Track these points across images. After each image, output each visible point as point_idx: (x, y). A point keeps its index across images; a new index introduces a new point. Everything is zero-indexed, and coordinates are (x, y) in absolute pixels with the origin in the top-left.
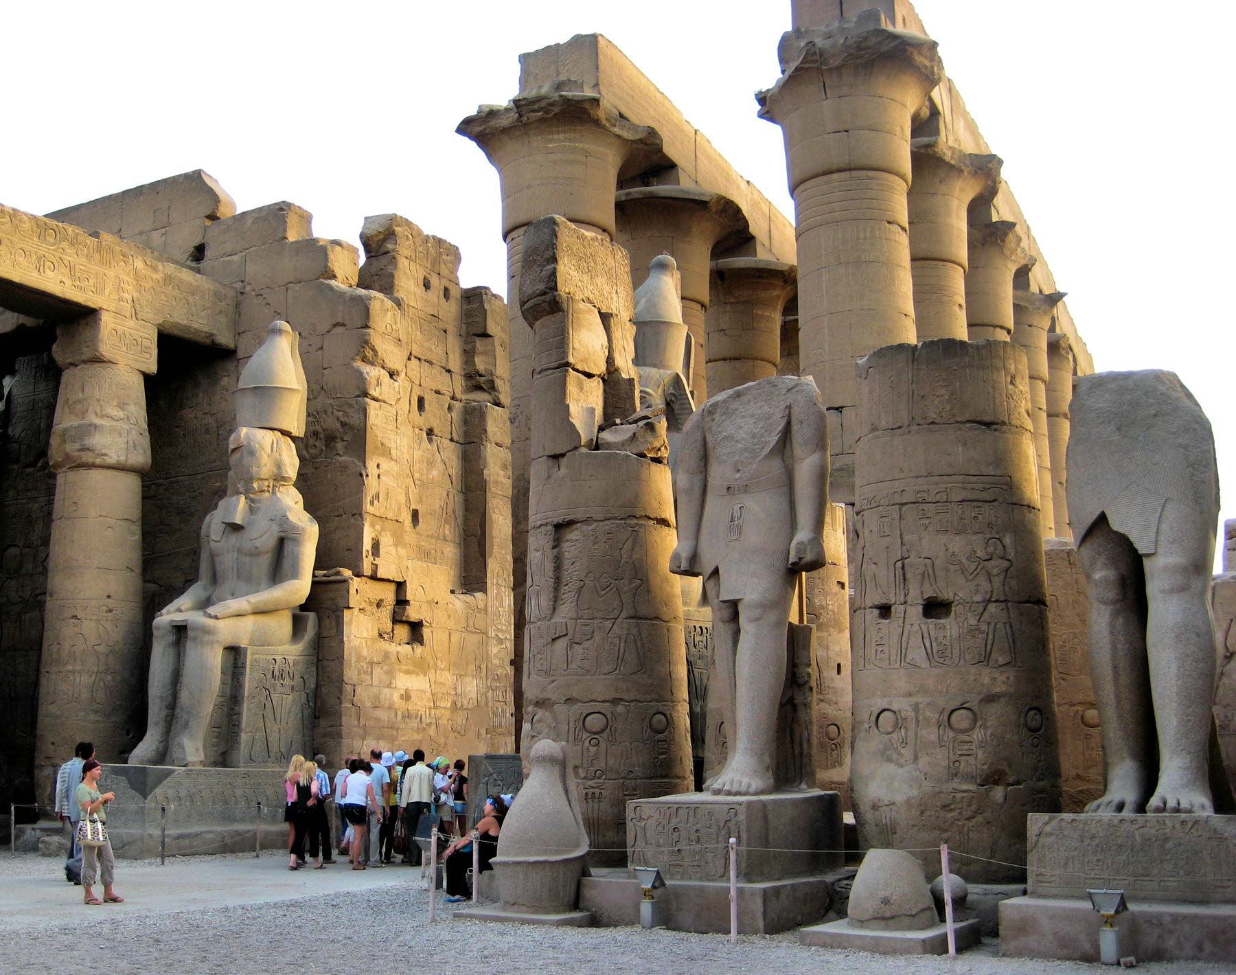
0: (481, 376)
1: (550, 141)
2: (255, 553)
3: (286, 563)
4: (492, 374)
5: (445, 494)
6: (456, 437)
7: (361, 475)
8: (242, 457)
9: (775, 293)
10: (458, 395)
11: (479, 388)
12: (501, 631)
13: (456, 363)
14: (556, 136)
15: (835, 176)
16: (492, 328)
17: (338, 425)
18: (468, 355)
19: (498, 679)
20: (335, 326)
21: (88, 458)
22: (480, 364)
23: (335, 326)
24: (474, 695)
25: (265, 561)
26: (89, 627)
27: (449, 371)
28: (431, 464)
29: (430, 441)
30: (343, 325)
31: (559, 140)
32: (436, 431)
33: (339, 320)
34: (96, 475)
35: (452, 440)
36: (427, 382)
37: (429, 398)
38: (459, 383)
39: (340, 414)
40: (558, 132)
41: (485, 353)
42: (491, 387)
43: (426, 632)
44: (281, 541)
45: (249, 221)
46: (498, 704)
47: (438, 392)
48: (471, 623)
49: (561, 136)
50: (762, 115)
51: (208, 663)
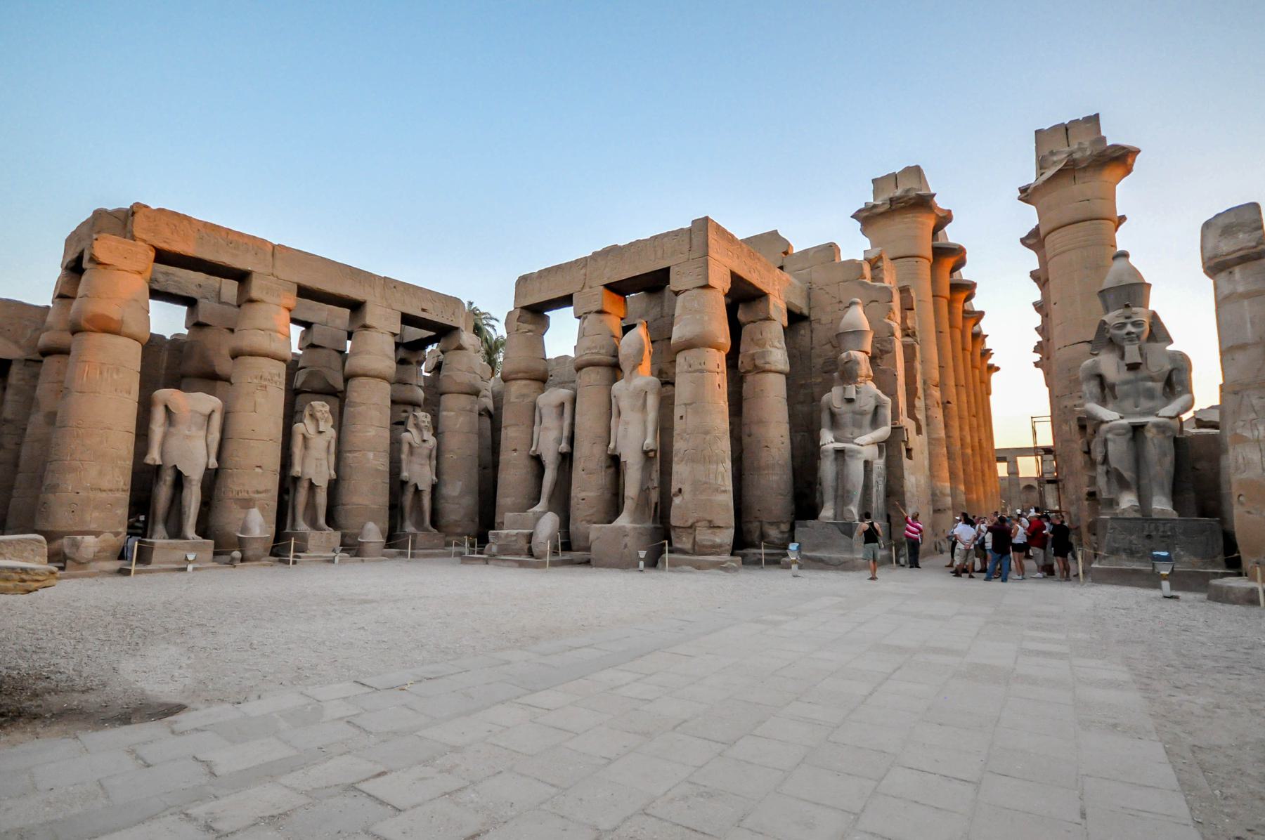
2: (863, 413)
3: (880, 418)
11: (908, 335)
21: (767, 367)
22: (909, 323)
25: (869, 417)
26: (774, 451)
34: (771, 377)
42: (914, 334)
43: (913, 454)
44: (877, 407)
45: (811, 253)
51: (856, 470)
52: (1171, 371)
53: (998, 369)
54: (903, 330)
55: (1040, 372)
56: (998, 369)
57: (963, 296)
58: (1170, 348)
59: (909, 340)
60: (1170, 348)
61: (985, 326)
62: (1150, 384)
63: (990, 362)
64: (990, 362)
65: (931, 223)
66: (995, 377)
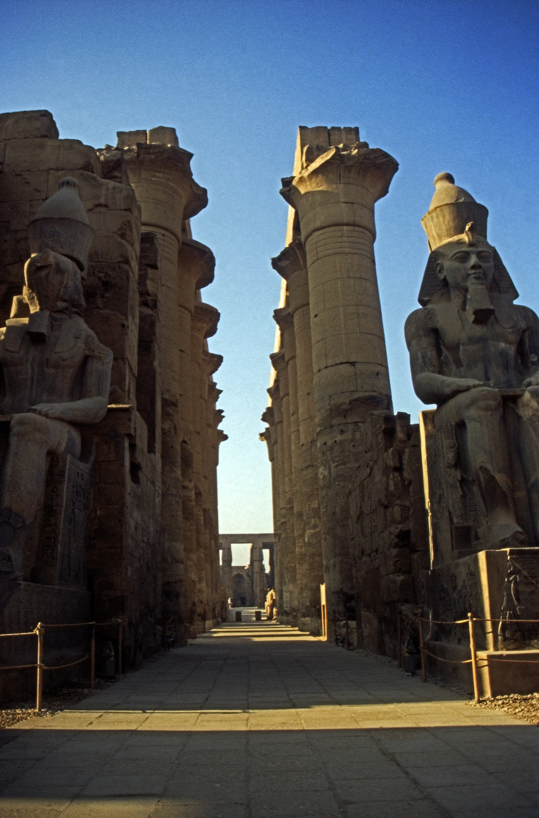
0: (149, 295)
1: (155, 176)
4: (156, 296)
7: (123, 326)
8: (48, 275)
9: (204, 325)
14: (158, 174)
15: (345, 228)
16: (159, 264)
17: (100, 284)
20: (97, 206)
22: (150, 286)
23: (97, 206)
30: (106, 206)
31: (160, 177)
33: (102, 201)
39: (102, 275)
40: (160, 172)
41: (152, 280)
44: (86, 359)
49: (161, 175)
50: (282, 193)
52: (524, 331)
53: (225, 438)
54: (141, 294)
55: (264, 444)
56: (225, 438)
57: (206, 327)
58: (516, 302)
59: (148, 311)
60: (516, 302)
61: (218, 378)
62: (503, 345)
63: (220, 427)
64: (220, 427)
65: (184, 198)
66: (223, 446)
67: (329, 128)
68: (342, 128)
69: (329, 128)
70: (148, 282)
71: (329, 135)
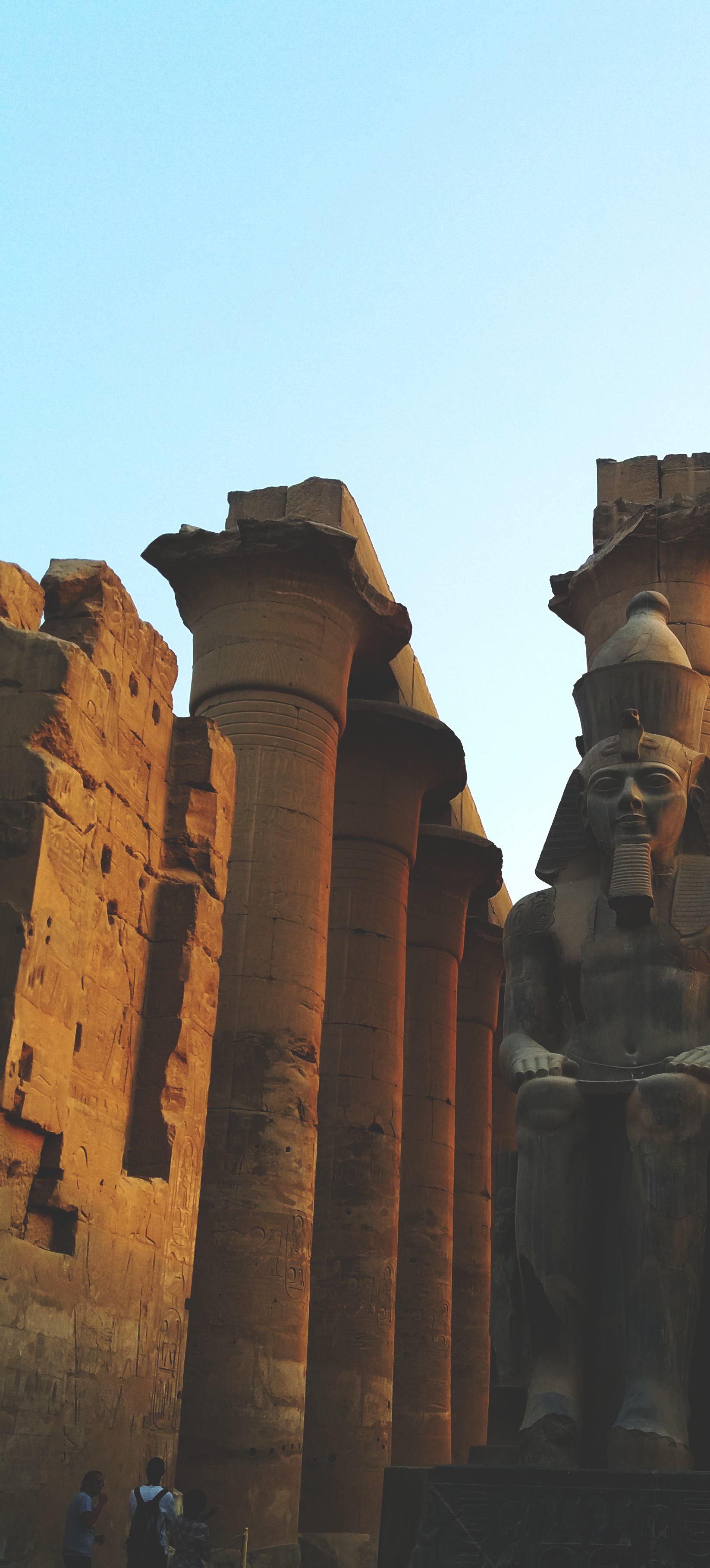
4: (207, 845)
5: (120, 1011)
6: (145, 929)
10: (155, 866)
12: (180, 1247)
13: (157, 817)
16: (217, 781)
18: (176, 812)
19: (167, 1331)
22: (193, 825)
24: (132, 1356)
27: (146, 826)
28: (107, 954)
29: (111, 921)
32: (121, 909)
35: (139, 930)
36: (118, 828)
37: (118, 855)
38: (156, 851)
41: (201, 813)
46: (162, 1374)
47: (130, 851)
48: (143, 1228)
67: (661, 458)
68: (689, 456)
69: (661, 458)
70: (189, 820)
71: (661, 473)
